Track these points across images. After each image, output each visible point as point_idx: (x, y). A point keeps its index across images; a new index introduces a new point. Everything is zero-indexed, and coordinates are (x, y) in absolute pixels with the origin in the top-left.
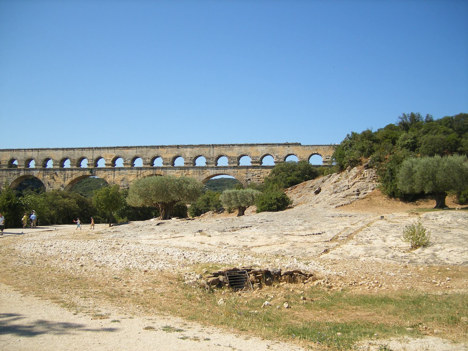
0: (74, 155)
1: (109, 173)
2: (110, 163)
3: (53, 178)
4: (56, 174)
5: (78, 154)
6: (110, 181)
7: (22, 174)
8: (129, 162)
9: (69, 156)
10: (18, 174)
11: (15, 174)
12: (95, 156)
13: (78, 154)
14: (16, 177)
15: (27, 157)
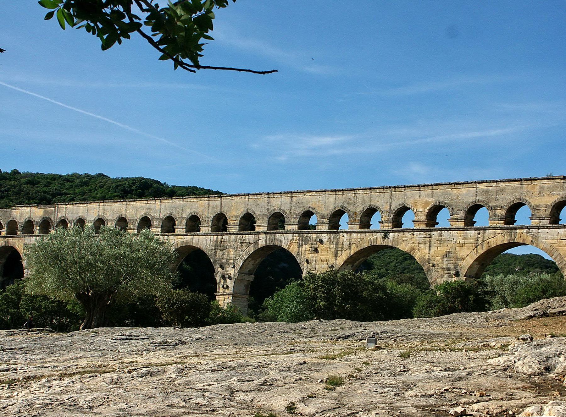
0: (354, 203)
1: (421, 241)
2: (423, 218)
3: (316, 251)
4: (321, 242)
5: (363, 201)
6: (422, 258)
7: (261, 243)
8: (461, 214)
9: (345, 205)
10: (256, 243)
11: (250, 243)
12: (396, 205)
13: (363, 201)
14: (252, 250)
15: (272, 209)
